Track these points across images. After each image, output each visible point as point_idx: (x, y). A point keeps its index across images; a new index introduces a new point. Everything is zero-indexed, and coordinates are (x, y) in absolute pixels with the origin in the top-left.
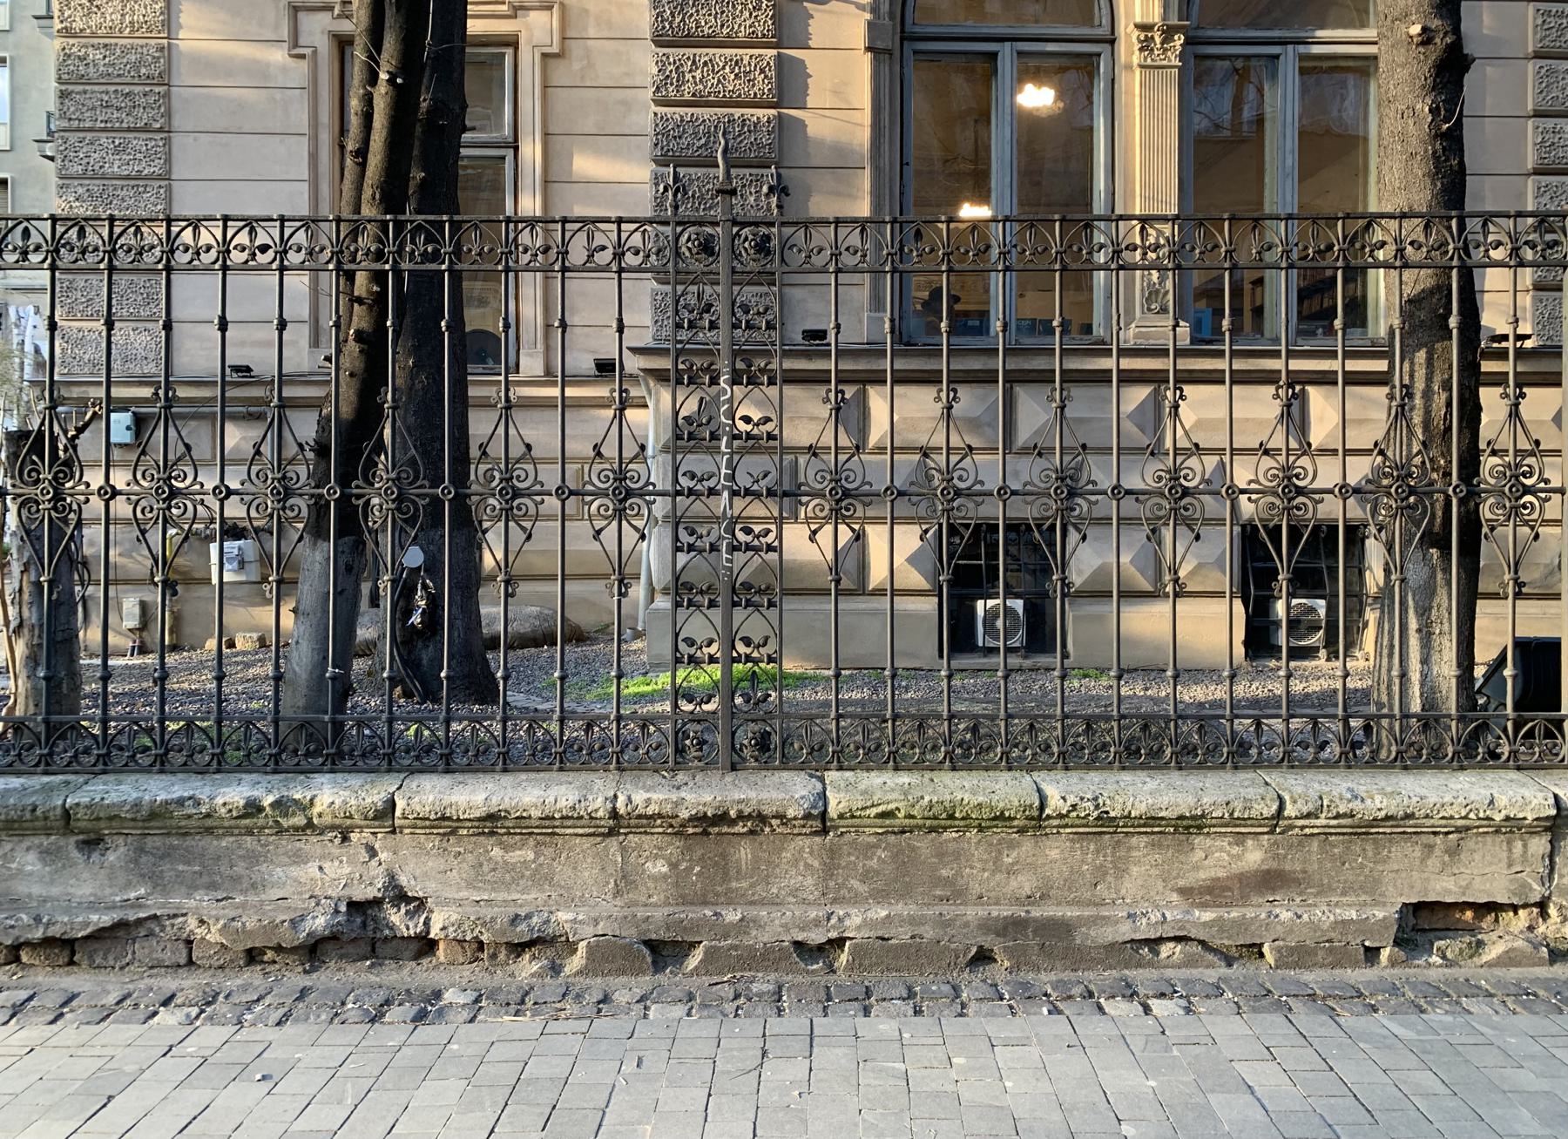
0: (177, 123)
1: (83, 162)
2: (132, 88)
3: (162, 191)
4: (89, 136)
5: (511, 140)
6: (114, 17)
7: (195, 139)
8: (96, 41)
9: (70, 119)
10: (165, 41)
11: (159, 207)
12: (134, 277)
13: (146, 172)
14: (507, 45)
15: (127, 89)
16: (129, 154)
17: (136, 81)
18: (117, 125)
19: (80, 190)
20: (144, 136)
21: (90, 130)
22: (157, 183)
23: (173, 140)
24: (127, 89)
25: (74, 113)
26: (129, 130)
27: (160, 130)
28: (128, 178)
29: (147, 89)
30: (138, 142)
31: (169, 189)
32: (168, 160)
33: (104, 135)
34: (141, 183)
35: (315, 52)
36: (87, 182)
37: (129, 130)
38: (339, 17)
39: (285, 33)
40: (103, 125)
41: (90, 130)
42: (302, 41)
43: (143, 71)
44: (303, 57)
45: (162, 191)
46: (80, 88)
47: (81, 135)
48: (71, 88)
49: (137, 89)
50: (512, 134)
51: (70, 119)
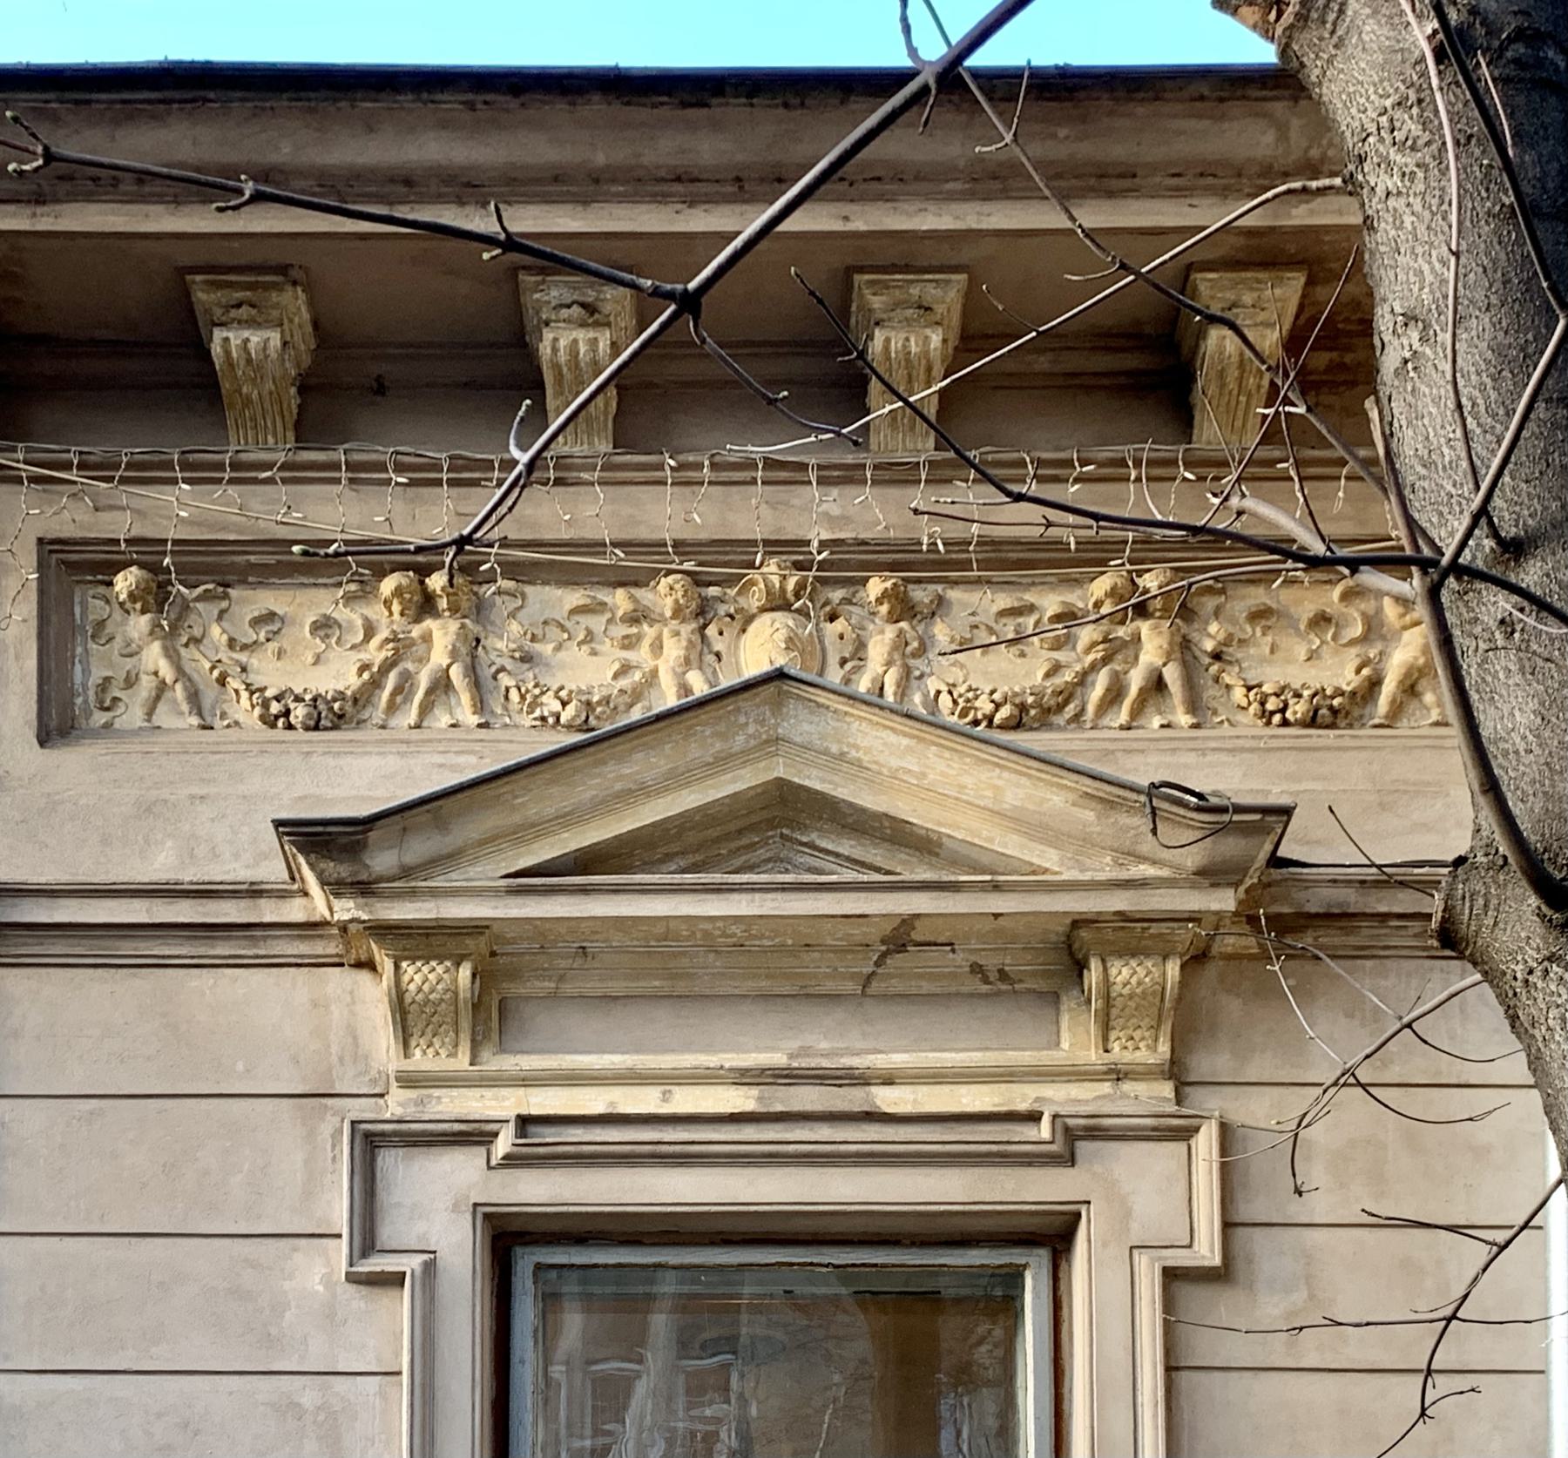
14: (1028, 1240)
35: (430, 1268)
38: (511, 1161)
39: (338, 1210)
42: (388, 1234)
44: (397, 1280)
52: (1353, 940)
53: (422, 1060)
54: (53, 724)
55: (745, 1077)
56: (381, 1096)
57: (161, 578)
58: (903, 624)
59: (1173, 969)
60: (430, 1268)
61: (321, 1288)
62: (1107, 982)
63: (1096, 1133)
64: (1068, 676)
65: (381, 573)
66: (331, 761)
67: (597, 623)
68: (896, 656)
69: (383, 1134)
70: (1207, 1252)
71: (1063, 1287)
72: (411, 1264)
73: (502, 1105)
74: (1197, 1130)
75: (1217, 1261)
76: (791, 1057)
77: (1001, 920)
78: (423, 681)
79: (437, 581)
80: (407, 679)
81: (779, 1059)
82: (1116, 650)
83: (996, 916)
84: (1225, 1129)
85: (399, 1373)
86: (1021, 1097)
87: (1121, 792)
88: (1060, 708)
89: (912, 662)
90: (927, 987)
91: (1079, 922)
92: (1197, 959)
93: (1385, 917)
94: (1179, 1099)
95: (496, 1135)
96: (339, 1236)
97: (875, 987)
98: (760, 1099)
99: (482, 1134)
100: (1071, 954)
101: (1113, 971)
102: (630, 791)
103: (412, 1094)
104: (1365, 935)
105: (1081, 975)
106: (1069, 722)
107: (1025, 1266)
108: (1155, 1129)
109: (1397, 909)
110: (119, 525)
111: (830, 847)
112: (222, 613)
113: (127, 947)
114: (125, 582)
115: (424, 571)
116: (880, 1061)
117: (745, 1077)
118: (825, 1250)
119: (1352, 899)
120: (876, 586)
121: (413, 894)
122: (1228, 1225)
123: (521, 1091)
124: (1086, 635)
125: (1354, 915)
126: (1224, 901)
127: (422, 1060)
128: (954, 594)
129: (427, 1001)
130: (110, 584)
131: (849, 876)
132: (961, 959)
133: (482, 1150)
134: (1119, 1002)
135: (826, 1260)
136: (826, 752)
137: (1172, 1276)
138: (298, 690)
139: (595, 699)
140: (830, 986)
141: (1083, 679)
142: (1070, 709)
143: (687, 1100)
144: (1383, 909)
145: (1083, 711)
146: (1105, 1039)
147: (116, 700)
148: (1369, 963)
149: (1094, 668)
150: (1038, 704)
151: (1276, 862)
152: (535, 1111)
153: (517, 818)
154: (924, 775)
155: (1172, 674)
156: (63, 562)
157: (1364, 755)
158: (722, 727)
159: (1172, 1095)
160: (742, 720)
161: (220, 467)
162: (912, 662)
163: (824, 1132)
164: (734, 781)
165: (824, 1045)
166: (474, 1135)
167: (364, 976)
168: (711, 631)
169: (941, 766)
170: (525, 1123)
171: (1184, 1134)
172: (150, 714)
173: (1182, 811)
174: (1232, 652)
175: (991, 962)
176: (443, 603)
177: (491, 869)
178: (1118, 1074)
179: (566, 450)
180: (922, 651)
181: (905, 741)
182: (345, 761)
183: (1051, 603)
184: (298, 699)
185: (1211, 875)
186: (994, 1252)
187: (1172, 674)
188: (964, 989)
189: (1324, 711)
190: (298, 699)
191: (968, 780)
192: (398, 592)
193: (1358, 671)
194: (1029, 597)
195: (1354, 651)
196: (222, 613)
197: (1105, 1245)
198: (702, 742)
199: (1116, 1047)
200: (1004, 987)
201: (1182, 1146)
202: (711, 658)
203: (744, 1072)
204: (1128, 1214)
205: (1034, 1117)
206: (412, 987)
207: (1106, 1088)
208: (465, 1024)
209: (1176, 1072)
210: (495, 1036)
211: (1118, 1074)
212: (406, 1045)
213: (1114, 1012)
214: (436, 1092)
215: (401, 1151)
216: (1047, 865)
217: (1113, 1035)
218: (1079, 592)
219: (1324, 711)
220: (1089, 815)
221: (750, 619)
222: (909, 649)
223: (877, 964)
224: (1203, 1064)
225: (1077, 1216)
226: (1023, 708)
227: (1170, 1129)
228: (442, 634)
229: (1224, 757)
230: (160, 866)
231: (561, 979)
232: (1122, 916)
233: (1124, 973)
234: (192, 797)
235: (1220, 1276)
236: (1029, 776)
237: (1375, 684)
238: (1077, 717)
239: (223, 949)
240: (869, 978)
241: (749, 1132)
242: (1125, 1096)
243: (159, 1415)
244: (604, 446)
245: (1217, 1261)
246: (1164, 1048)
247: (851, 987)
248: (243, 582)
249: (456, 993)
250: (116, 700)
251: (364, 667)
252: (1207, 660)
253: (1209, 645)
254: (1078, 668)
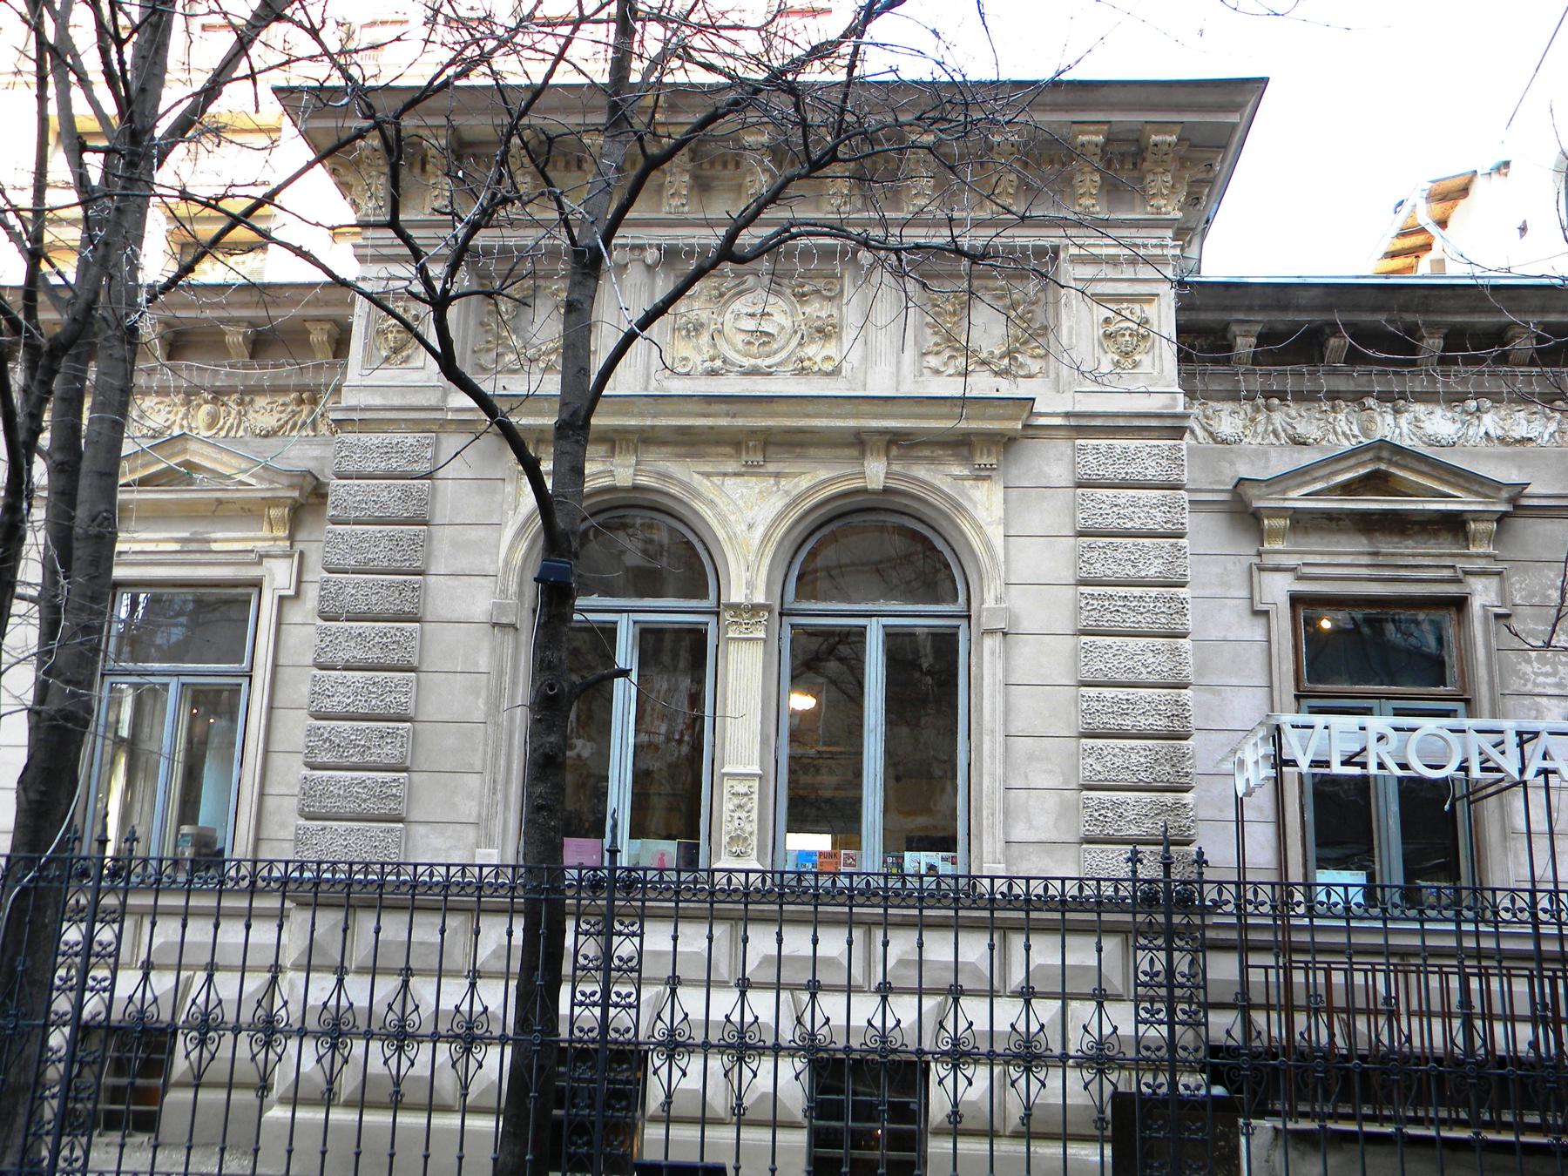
55: (177, 540)
63: (268, 556)
81: (186, 535)
86: (249, 546)
116: (213, 536)
117: (177, 540)
132: (237, 506)
163: (198, 556)
171: (291, 556)
178: (275, 539)
205: (252, 551)
211: (275, 539)
224: (300, 536)
241: (179, 556)
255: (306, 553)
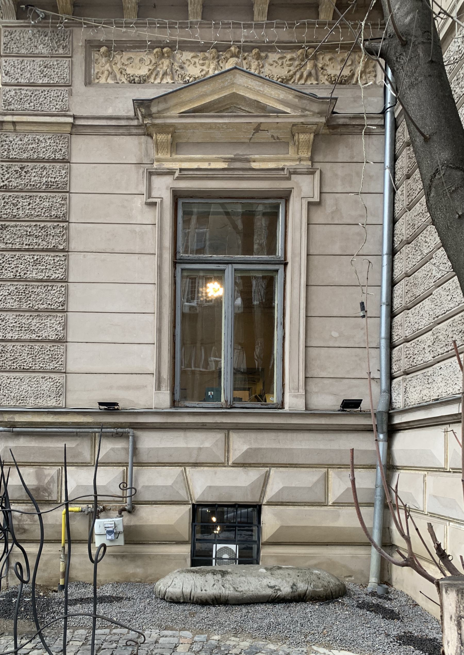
0: (73, 245)
1: (14, 271)
2: (46, 224)
3: (63, 289)
4: (18, 254)
5: (283, 259)
6: (36, 178)
7: (84, 256)
8: (24, 194)
9: (7, 243)
10: (68, 194)
11: (61, 299)
12: (44, 344)
13: (53, 277)
15: (42, 224)
16: (43, 265)
17: (48, 219)
18: (36, 247)
19: (12, 288)
20: (52, 254)
21: (19, 250)
22: (60, 284)
23: (70, 257)
24: (42, 224)
25: (9, 239)
26: (43, 250)
27: (63, 250)
28: (41, 281)
29: (56, 224)
30: (48, 258)
31: (67, 288)
32: (67, 270)
33: (27, 253)
34: (50, 284)
35: (162, 201)
36: (16, 283)
37: (43, 250)
38: (178, 178)
39: (143, 189)
40: (27, 247)
41: (19, 250)
42: (154, 194)
43: (53, 213)
45: (63, 289)
46: (13, 224)
47: (14, 253)
48: (7, 223)
49: (49, 224)
50: (283, 256)
51: (7, 243)
52: (348, 131)
53: (160, 156)
54: (88, 82)
56: (152, 164)
57: (110, 49)
58: (259, 61)
59: (312, 136)
60: (162, 201)
61: (140, 206)
62: (299, 139)
63: (295, 173)
64: (291, 73)
65: (154, 49)
66: (143, 90)
67: (196, 60)
68: (258, 67)
69: (152, 172)
70: (316, 199)
71: (287, 208)
72: (158, 201)
73: (176, 166)
74: (316, 172)
75: (318, 200)
76: (235, 156)
77: (278, 124)
78: (161, 73)
79: (165, 50)
80: (158, 72)
81: (232, 156)
82: (301, 66)
83: (277, 123)
84: (321, 171)
85: (155, 224)
87: (304, 95)
88: (290, 80)
89: (261, 69)
90: (262, 141)
91: (294, 125)
92: (316, 135)
93: (354, 125)
94: (312, 166)
95: (175, 172)
96: (143, 194)
97: (252, 141)
98: (228, 165)
99: (172, 172)
100: (292, 133)
101: (300, 136)
102: (203, 95)
103: (158, 163)
104: (351, 129)
105: (293, 138)
106: (292, 83)
107: (280, 203)
108: (307, 172)
109: (357, 123)
110: (102, 38)
111: (244, 109)
112: (121, 57)
113: (102, 130)
114: (103, 49)
115: (163, 48)
116: (253, 157)
118: (240, 199)
119: (348, 121)
120: (255, 51)
121: (159, 118)
122: (321, 193)
123: (180, 163)
124: (297, 63)
125: (348, 125)
126: (323, 120)
127: (160, 156)
128: (270, 54)
129: (162, 142)
130: (99, 51)
131: (248, 114)
132: (269, 134)
133: (172, 176)
134: (301, 143)
135: (240, 202)
136: (244, 86)
137: (309, 204)
138: (136, 75)
139: (196, 77)
140: (243, 140)
141: (295, 74)
142: (292, 80)
143: (214, 165)
144: (354, 123)
145: (295, 80)
146: (298, 152)
147: (100, 77)
148: (351, 136)
149: (297, 70)
150: (286, 79)
151: (333, 113)
152: (183, 167)
153: (181, 100)
154: (264, 91)
155: (313, 72)
156: (91, 46)
157: (351, 90)
158: (223, 80)
159: (310, 164)
160: (227, 78)
161: (122, 23)
162: (261, 69)
163: (241, 173)
164: (225, 93)
165: (241, 153)
166: (170, 172)
167: (149, 139)
168: (220, 62)
169: (268, 90)
170: (181, 170)
171: (313, 173)
172: (107, 80)
173: (315, 99)
174: (325, 68)
175: (275, 135)
176: (166, 55)
177: (175, 112)
178: (300, 160)
179: (192, 20)
180: (263, 67)
181: (260, 84)
182: (146, 90)
183: (289, 56)
184: (136, 77)
185: (320, 114)
186: (274, 200)
187: (313, 72)
188: (270, 141)
189: (343, 81)
190: (136, 77)
191: (273, 93)
192: (157, 52)
193: (350, 72)
194: (285, 55)
195: (349, 67)
196: (121, 57)
197: (296, 197)
198: (218, 83)
199: (300, 153)
200: (278, 141)
201: (312, 176)
202: (220, 68)
203: (225, 159)
204: (301, 190)
205: (283, 169)
206: (159, 139)
207: (298, 163)
208: (169, 148)
209: (312, 159)
210: (175, 150)
212: (157, 152)
213: (300, 145)
214: (163, 163)
215: (156, 176)
216: (288, 112)
217: (300, 151)
218: (295, 54)
219: (343, 81)
220: (297, 100)
221: (228, 59)
222: (260, 66)
223: (253, 135)
224: (318, 158)
225: (291, 191)
226: (283, 79)
227: (310, 172)
228: (166, 62)
229: (323, 90)
230: (110, 112)
231: (189, 138)
232: (302, 123)
233: (302, 137)
234: (115, 98)
235: (319, 204)
236: (285, 91)
237: (353, 75)
238: (293, 82)
239: (121, 131)
240: (251, 138)
242: (301, 165)
243: (108, 232)
244: (199, 19)
245: (318, 200)
246: (310, 154)
247: (247, 141)
248: (126, 50)
249: (168, 140)
250: (100, 77)
251: (149, 70)
252: (320, 69)
253: (320, 65)
254: (294, 71)
255: (324, 172)
